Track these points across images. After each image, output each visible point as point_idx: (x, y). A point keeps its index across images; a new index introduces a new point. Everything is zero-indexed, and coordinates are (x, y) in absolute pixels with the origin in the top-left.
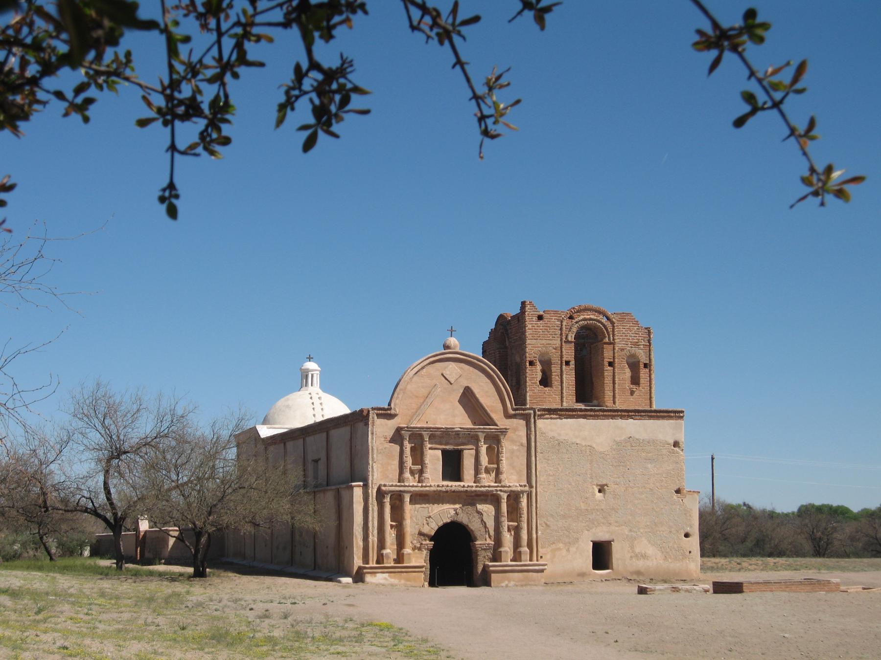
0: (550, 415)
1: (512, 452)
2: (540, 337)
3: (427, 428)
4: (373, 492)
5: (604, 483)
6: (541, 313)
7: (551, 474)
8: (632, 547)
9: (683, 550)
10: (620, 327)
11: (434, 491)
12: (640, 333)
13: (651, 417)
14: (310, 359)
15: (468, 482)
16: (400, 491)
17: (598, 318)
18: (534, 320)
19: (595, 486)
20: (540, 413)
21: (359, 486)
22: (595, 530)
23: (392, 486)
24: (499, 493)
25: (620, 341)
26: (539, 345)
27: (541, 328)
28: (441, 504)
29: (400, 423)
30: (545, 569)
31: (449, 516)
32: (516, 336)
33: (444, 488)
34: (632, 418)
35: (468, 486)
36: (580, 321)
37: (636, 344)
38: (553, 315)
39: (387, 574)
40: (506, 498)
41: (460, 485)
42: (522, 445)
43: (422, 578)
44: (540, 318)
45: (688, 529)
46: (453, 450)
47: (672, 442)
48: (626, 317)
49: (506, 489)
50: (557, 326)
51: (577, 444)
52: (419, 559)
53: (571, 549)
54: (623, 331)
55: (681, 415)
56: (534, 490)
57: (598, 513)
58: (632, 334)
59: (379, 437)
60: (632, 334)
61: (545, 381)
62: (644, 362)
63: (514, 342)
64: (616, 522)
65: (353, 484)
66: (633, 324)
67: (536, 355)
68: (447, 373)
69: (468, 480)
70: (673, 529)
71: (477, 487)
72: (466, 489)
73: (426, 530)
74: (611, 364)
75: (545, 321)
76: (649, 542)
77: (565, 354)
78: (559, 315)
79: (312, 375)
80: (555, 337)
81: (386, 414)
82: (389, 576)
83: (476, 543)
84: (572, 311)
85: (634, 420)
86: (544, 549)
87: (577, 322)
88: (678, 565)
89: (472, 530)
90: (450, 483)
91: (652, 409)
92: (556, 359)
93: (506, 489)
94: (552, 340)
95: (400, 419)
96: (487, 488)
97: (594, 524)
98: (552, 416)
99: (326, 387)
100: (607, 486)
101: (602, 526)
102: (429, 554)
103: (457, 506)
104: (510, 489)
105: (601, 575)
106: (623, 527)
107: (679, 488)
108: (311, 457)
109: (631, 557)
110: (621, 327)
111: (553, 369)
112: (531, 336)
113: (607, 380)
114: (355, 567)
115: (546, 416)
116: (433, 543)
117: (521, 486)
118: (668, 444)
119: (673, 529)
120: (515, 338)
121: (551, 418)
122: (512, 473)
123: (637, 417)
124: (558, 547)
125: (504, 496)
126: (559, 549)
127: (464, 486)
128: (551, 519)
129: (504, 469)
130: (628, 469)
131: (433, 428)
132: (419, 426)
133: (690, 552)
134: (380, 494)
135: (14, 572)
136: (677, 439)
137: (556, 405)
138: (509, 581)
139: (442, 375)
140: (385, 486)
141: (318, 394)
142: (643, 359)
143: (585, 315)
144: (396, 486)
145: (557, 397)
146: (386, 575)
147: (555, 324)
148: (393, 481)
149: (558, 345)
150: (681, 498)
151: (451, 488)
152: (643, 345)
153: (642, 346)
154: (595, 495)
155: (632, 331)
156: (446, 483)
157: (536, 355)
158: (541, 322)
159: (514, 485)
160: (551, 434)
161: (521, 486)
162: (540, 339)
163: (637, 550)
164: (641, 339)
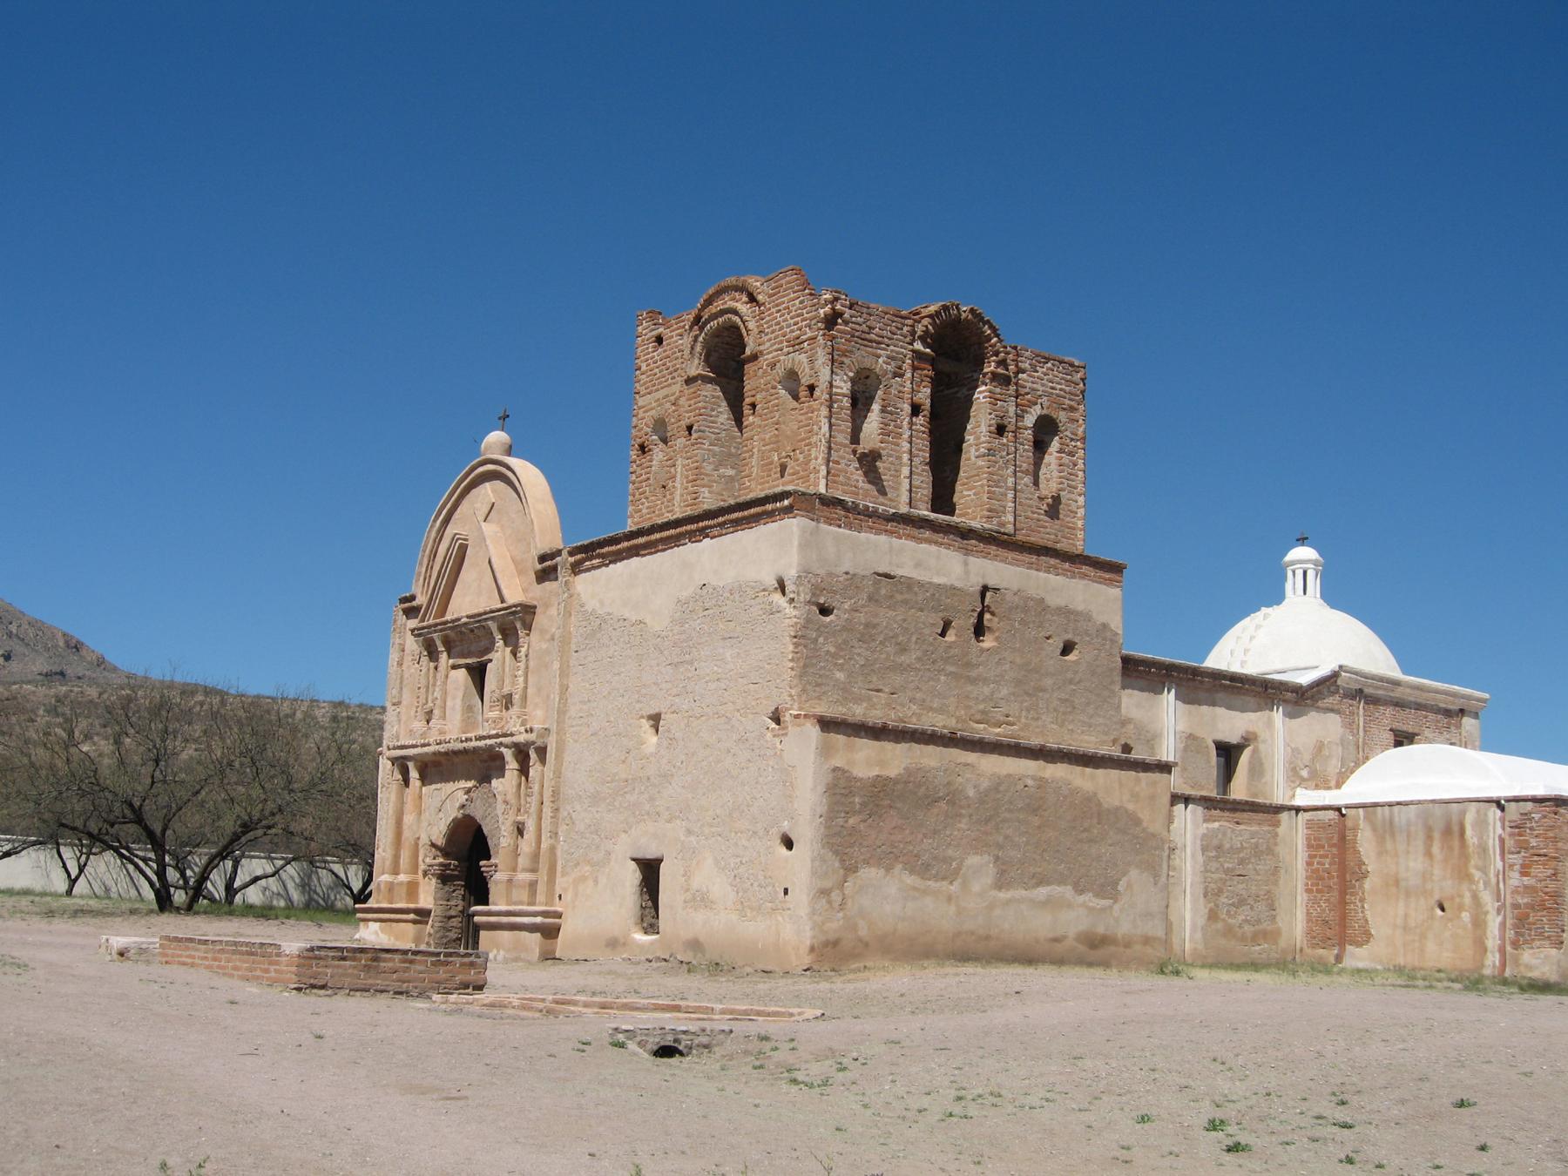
11: (434, 754)
12: (804, 311)
13: (738, 524)
14: (1302, 541)
19: (644, 721)
25: (771, 346)
28: (452, 783)
33: (442, 746)
34: (707, 536)
66: (794, 292)
79: (1305, 573)
83: (482, 863)
85: (712, 538)
99: (1334, 595)
103: (470, 784)
115: (587, 563)
118: (764, 590)
123: (715, 531)
133: (786, 892)
135: (303, 922)
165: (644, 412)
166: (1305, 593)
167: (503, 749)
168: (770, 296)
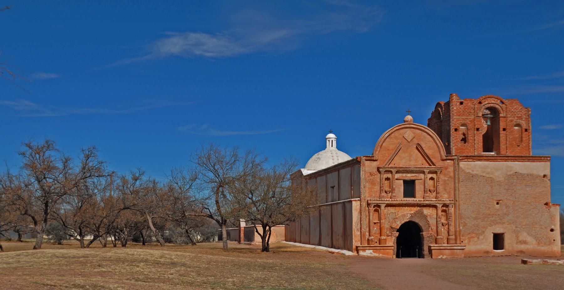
0: (468, 159)
1: (445, 181)
2: (461, 114)
3: (395, 167)
4: (364, 204)
5: (500, 199)
6: (462, 101)
7: (468, 194)
8: (517, 237)
9: (550, 239)
10: (510, 108)
15: (418, 199)
16: (379, 203)
17: (497, 103)
18: (458, 105)
20: (461, 158)
21: (356, 200)
22: (495, 226)
23: (375, 200)
24: (436, 204)
26: (461, 119)
27: (462, 109)
29: (379, 165)
30: (465, 249)
31: (408, 218)
32: (447, 114)
33: (404, 202)
34: (517, 161)
35: (419, 201)
36: (486, 104)
37: (520, 118)
38: (469, 101)
39: (372, 250)
40: (440, 207)
41: (414, 200)
42: (450, 177)
43: (391, 253)
44: (461, 103)
45: (553, 227)
46: (410, 180)
47: (542, 174)
48: (514, 102)
49: (441, 202)
50: (472, 108)
51: (483, 176)
52: (391, 242)
53: (480, 237)
54: (512, 110)
55: (549, 159)
56: (457, 203)
57: (497, 217)
58: (518, 111)
59: (367, 173)
60: (518, 111)
61: (464, 140)
62: (525, 128)
63: (446, 118)
64: (508, 222)
65: (352, 199)
67: (459, 125)
68: (406, 136)
69: (419, 197)
70: (543, 227)
71: (424, 201)
72: (417, 202)
73: (394, 225)
74: (504, 130)
75: (464, 105)
76: (528, 234)
77: (477, 124)
78: (473, 102)
79: (332, 141)
80: (470, 114)
81: (371, 159)
82: (373, 251)
84: (480, 99)
86: (464, 237)
87: (484, 105)
88: (546, 248)
89: (420, 226)
90: (408, 199)
91: (530, 156)
92: (471, 126)
93: (441, 202)
94: (468, 116)
95: (379, 162)
96: (430, 202)
97: (494, 223)
98: (469, 160)
100: (502, 201)
101: (498, 224)
102: (396, 239)
104: (443, 202)
105: (498, 253)
106: (512, 225)
107: (547, 202)
108: (330, 185)
109: (517, 242)
110: (511, 108)
111: (469, 133)
112: (456, 114)
113: (501, 139)
114: (353, 247)
116: (398, 233)
117: (450, 200)
119: (543, 227)
120: (447, 115)
121: (468, 161)
122: (444, 194)
124: (472, 236)
125: (439, 206)
126: (473, 237)
127: (416, 201)
128: (468, 220)
129: (440, 191)
130: (515, 191)
131: (398, 167)
132: (389, 166)
133: (554, 240)
134: (368, 205)
136: (546, 173)
137: (471, 154)
138: (443, 256)
139: (403, 137)
140: (370, 200)
141: (335, 151)
142: (524, 126)
143: (488, 101)
144: (377, 200)
145: (471, 149)
146: (371, 251)
147: (470, 107)
148: (375, 198)
149: (472, 119)
150: (548, 208)
151: (409, 202)
152: (525, 118)
153: (524, 119)
154: (495, 206)
155: (517, 110)
156: (405, 199)
157: (459, 125)
158: (462, 106)
159: (445, 200)
160: (467, 171)
161: (450, 200)
162: (461, 116)
163: (521, 238)
164: (523, 115)
165: (456, 120)
166: (332, 146)
167: (438, 205)
168: (509, 104)
